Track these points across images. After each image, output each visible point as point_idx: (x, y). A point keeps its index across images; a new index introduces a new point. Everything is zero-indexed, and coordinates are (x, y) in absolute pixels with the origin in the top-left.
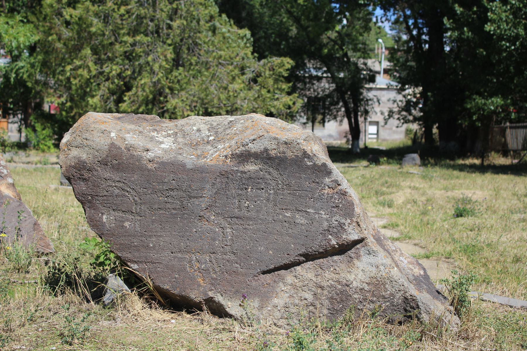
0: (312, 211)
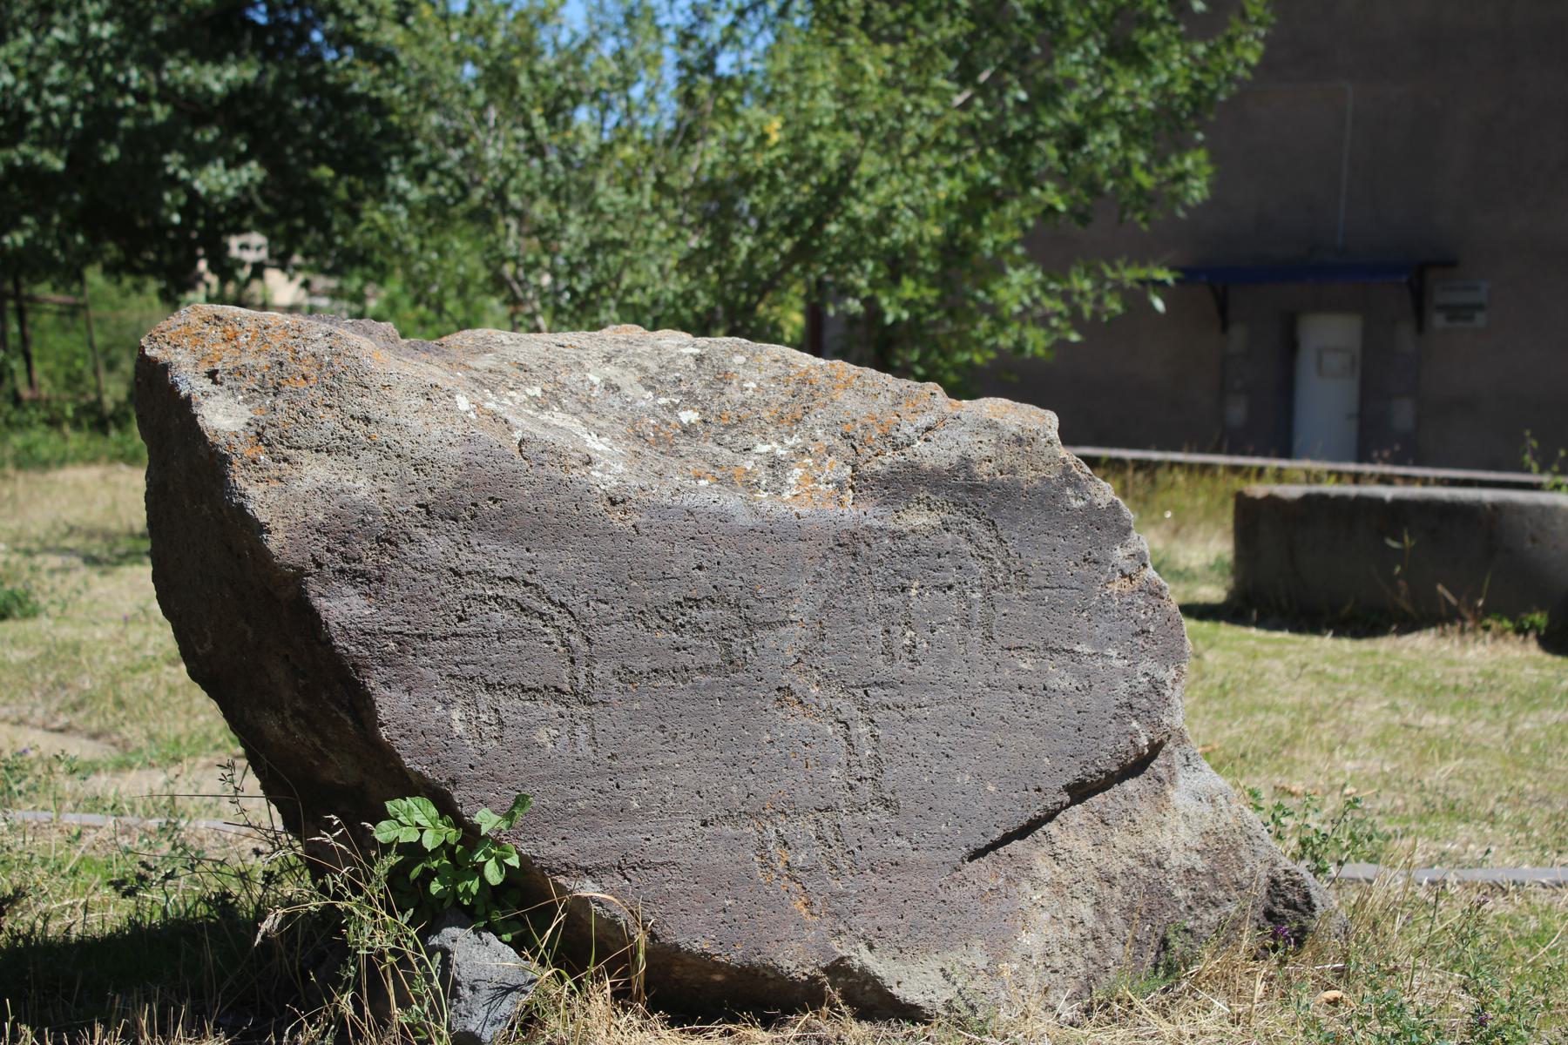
0: (1088, 650)
